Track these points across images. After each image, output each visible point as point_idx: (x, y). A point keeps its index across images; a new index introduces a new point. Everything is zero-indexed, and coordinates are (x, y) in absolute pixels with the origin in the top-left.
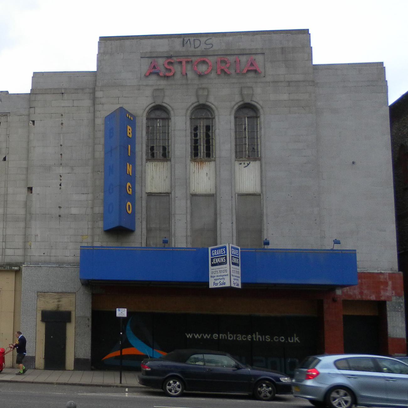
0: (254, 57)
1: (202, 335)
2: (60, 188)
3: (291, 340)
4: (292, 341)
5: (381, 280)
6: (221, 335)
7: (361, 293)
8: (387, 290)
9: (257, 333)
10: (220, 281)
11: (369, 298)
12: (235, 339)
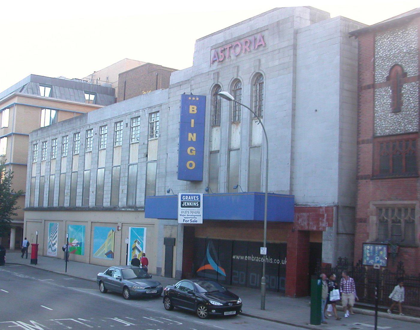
0: (263, 33)
3: (283, 263)
4: (284, 264)
5: (320, 213)
7: (308, 224)
8: (323, 221)
10: (191, 219)
11: (312, 229)
12: (255, 260)
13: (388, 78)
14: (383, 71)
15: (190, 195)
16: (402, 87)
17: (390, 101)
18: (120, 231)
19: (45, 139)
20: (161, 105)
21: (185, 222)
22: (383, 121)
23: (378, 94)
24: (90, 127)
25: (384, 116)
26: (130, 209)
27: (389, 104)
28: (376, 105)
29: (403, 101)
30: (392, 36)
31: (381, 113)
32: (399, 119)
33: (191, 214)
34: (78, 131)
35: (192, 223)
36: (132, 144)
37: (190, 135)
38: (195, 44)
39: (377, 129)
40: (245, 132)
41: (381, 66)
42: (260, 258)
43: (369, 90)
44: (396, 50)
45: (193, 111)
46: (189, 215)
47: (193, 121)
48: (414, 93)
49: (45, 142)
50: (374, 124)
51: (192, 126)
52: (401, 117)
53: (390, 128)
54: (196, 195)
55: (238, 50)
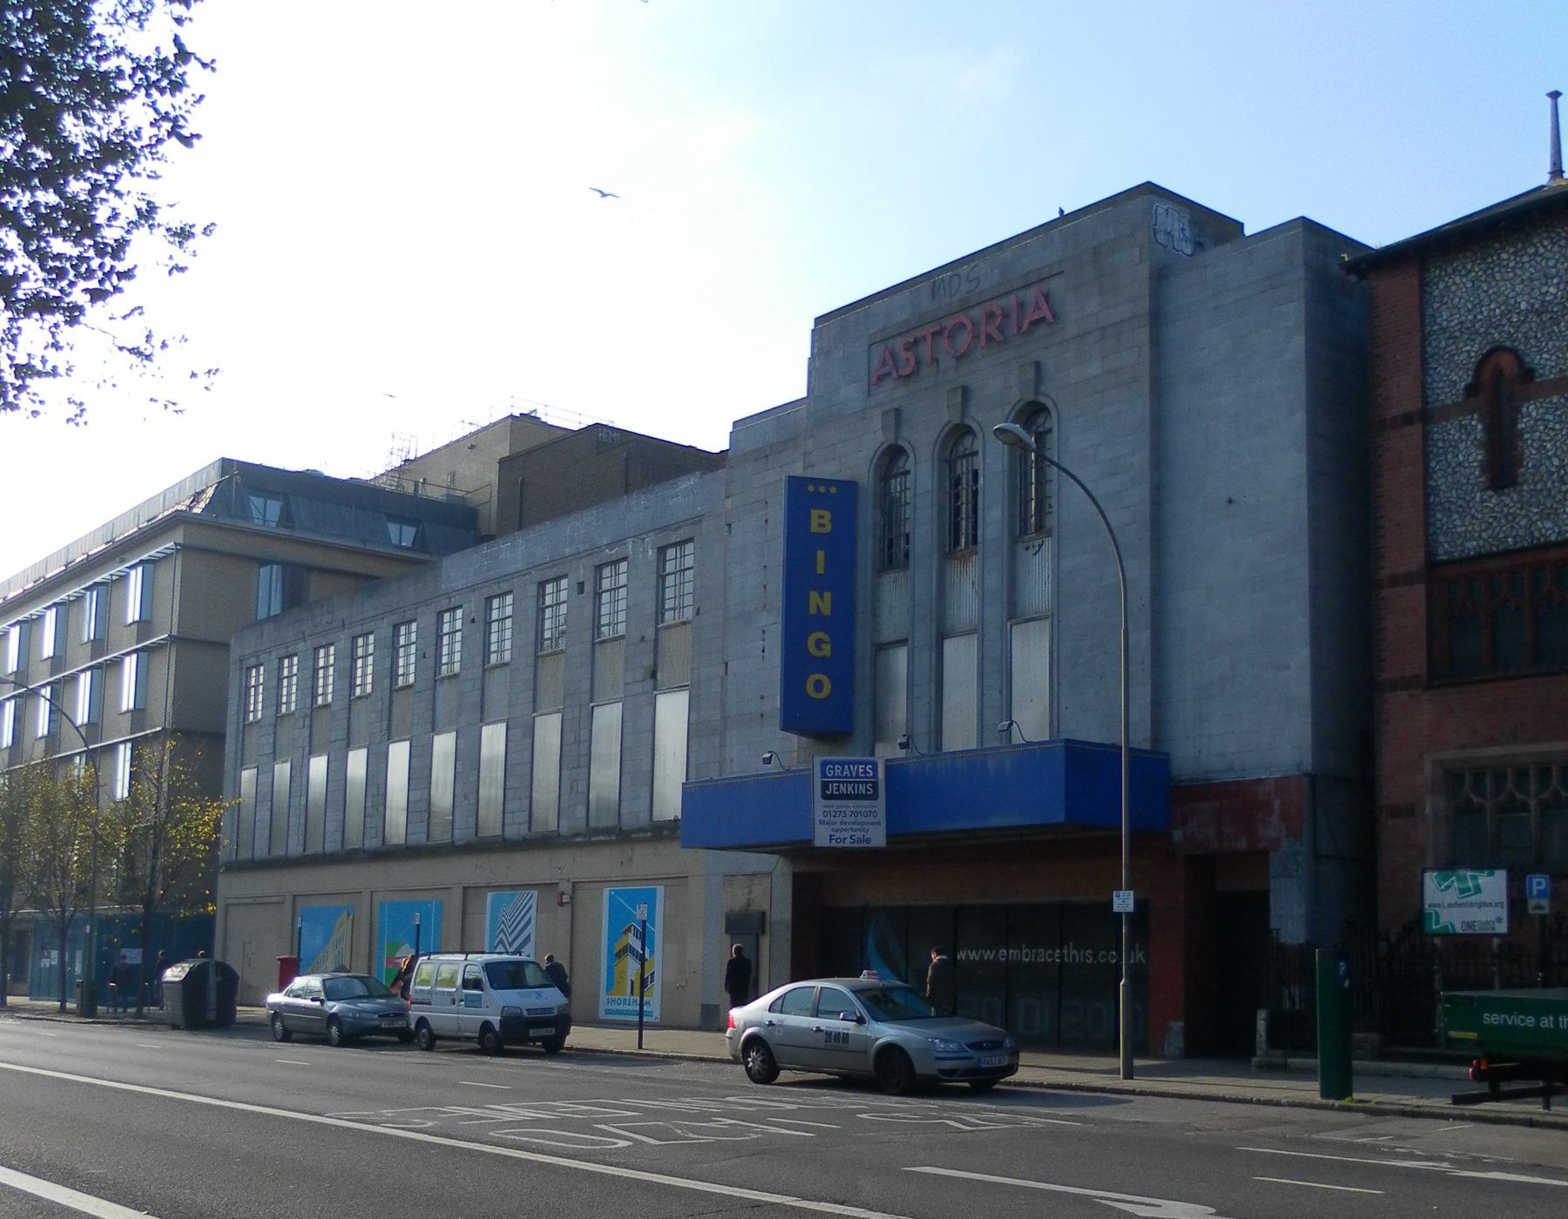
0: (1045, 286)
1: (981, 954)
2: (763, 658)
6: (1011, 951)
9: (1071, 944)
10: (853, 833)
12: (1033, 960)
13: (1472, 390)
14: (1451, 371)
15: (849, 763)
16: (1518, 409)
17: (1478, 456)
18: (568, 907)
19: (288, 647)
20: (698, 520)
21: (834, 844)
22: (1455, 516)
23: (1438, 440)
24: (450, 602)
25: (1460, 502)
26: (602, 838)
27: (1475, 464)
28: (1431, 470)
29: (1523, 453)
30: (1479, 264)
31: (1449, 494)
32: (1511, 508)
33: (853, 819)
34: (409, 615)
35: (856, 845)
36: (603, 642)
37: (814, 596)
38: (813, 331)
39: (1436, 541)
40: (994, 580)
41: (1447, 356)
42: (1050, 951)
43: (1409, 429)
44: (1492, 306)
45: (822, 525)
46: (846, 823)
47: (821, 555)
48: (1557, 426)
49: (288, 657)
50: (1427, 525)
51: (820, 569)
52: (1516, 502)
53: (1480, 536)
54: (866, 764)
55: (963, 339)
